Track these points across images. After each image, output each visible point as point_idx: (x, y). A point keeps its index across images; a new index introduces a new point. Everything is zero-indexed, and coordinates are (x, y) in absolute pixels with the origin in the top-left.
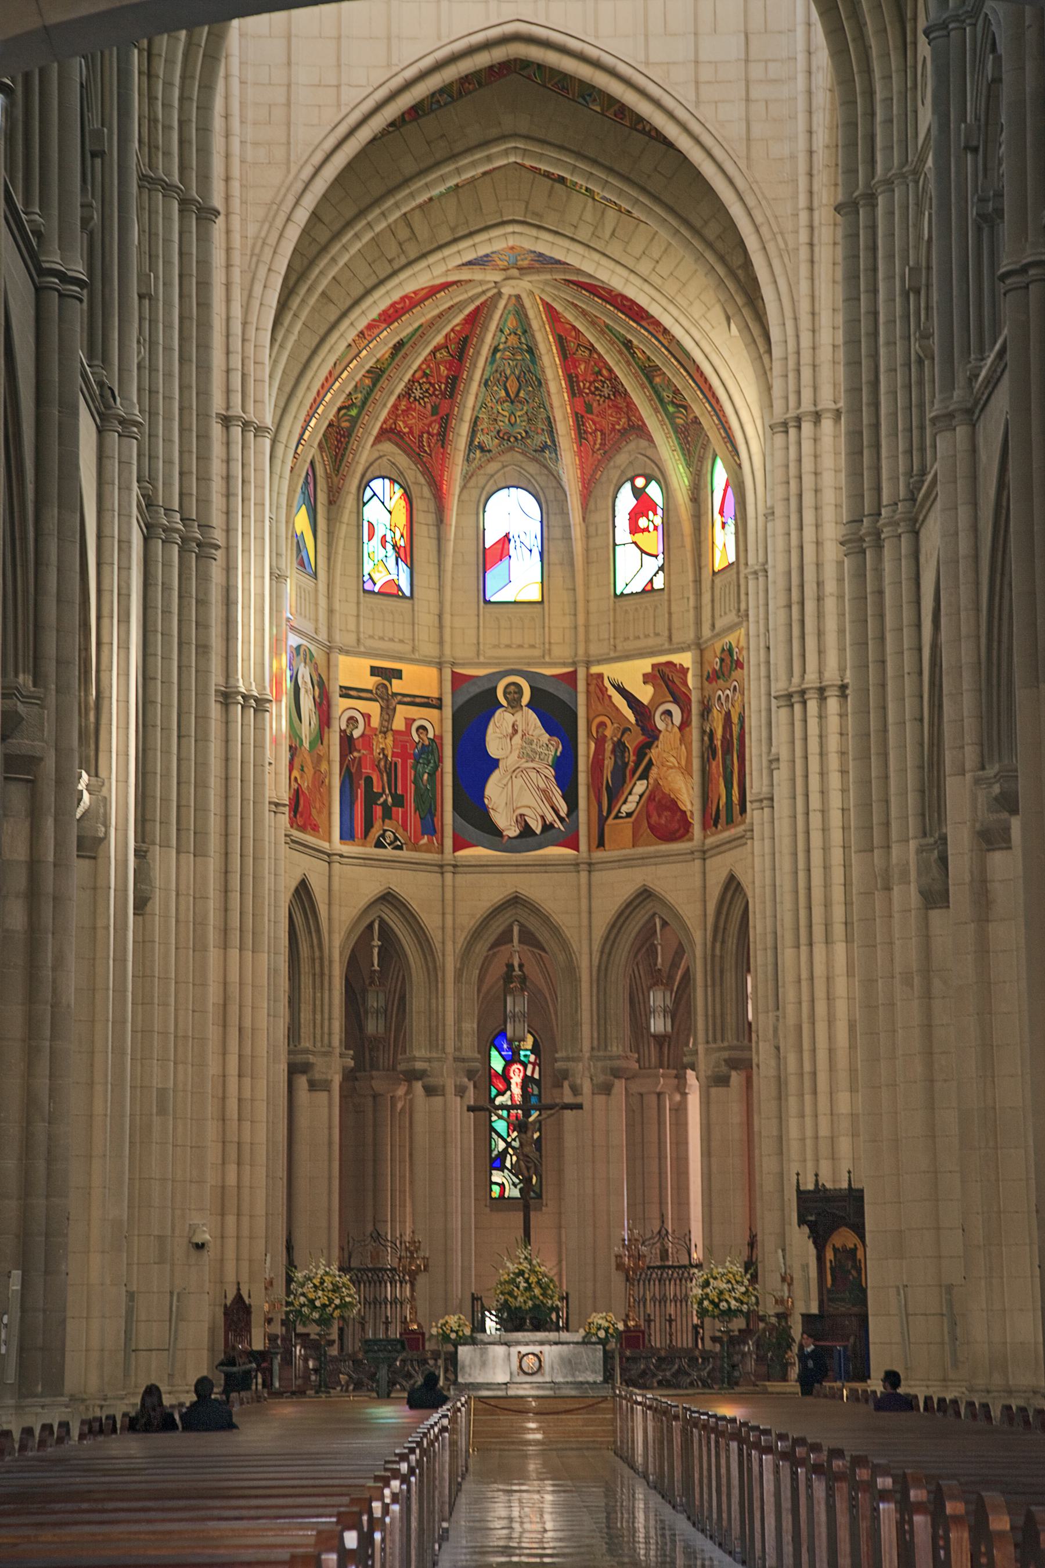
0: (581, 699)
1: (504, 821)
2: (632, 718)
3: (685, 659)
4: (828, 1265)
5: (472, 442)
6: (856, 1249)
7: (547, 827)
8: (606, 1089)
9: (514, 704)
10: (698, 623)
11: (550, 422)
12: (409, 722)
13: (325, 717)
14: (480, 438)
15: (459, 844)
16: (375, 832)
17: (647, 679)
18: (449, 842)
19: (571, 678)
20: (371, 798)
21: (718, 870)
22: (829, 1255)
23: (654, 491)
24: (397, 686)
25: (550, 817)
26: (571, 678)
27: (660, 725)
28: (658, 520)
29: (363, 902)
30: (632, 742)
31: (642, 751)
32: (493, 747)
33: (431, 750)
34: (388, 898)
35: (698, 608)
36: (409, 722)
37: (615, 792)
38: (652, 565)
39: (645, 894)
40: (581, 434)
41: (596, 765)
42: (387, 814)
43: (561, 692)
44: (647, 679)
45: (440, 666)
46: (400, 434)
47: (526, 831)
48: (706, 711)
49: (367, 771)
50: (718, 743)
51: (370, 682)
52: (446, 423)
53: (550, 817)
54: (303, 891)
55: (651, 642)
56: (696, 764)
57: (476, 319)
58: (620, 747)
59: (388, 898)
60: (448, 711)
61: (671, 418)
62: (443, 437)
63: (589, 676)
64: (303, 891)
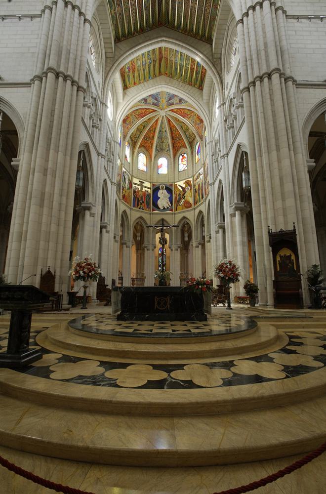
0: (173, 188)
1: (161, 207)
2: (182, 190)
3: (191, 179)
4: (278, 262)
5: (156, 149)
6: (291, 255)
7: (168, 208)
8: (177, 250)
9: (163, 189)
10: (193, 173)
11: (169, 145)
12: (145, 190)
13: (131, 187)
14: (158, 148)
15: (153, 210)
16: (139, 206)
17: (184, 183)
18: (151, 210)
19: (172, 185)
20: (138, 201)
21: (197, 211)
22: (278, 259)
23: (185, 155)
24: (143, 184)
25: (168, 206)
26: (172, 185)
27: (186, 190)
28: (186, 159)
29: (137, 217)
30: (182, 194)
31: (183, 195)
32: (159, 196)
33: (149, 195)
34: (141, 218)
35: (193, 171)
36: (145, 190)
37: (179, 202)
38: (185, 166)
39: (184, 218)
40: (174, 147)
41: (176, 198)
42: (141, 204)
43: (170, 187)
44: (184, 183)
45: (151, 183)
46: (145, 147)
47: (164, 208)
48: (194, 186)
49: (138, 196)
50: (197, 190)
51: (139, 183)
52: (152, 144)
53: (168, 206)
54: (125, 212)
55: (185, 178)
56: (193, 195)
57: (157, 121)
58: (180, 194)
59: (141, 218)
60: (152, 189)
61: (189, 140)
62: (152, 147)
63: (174, 185)
64: (125, 212)
